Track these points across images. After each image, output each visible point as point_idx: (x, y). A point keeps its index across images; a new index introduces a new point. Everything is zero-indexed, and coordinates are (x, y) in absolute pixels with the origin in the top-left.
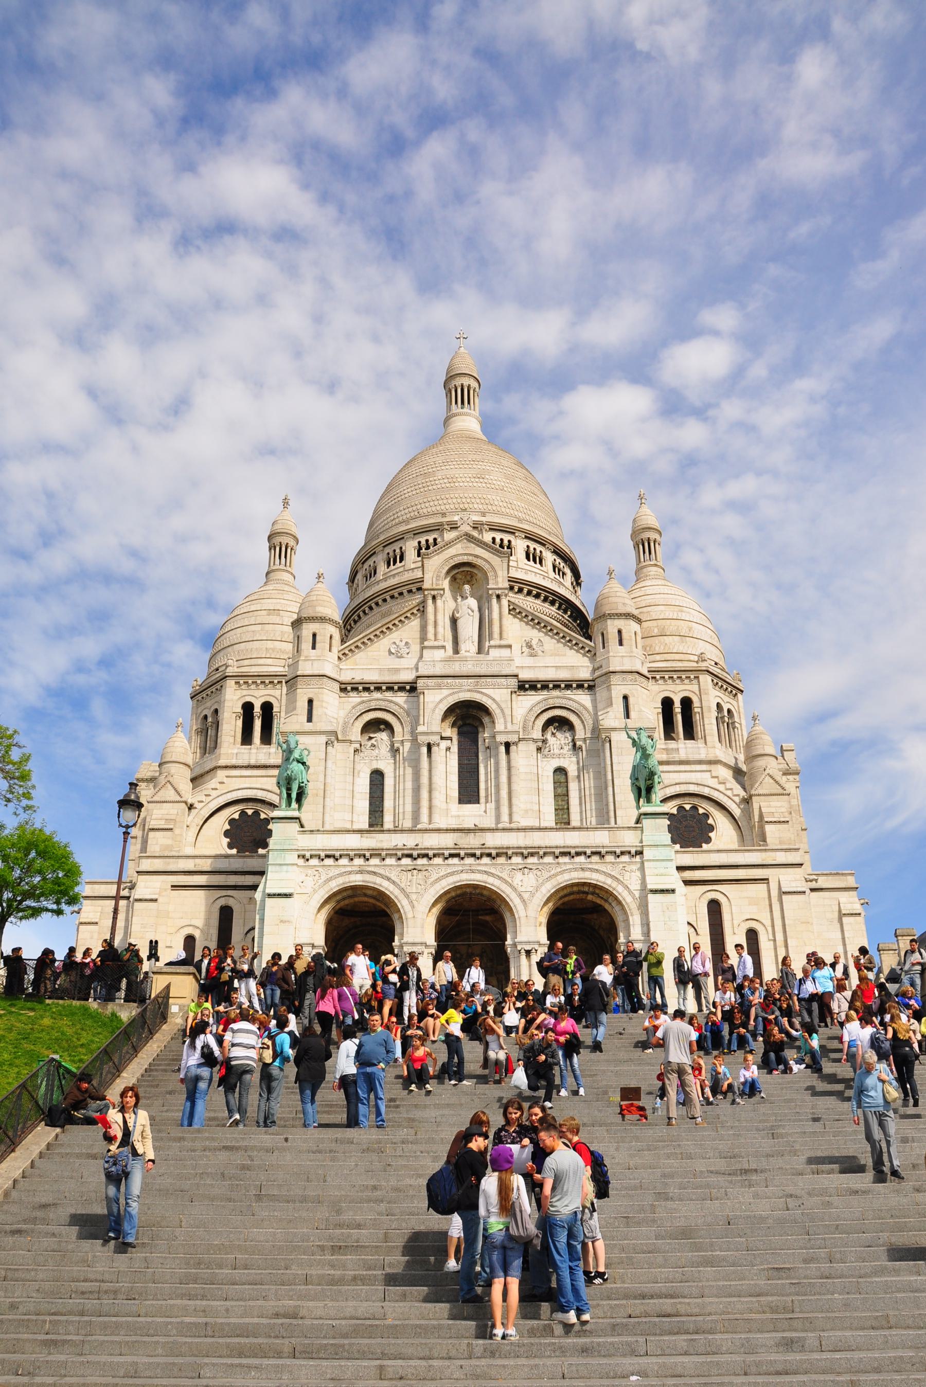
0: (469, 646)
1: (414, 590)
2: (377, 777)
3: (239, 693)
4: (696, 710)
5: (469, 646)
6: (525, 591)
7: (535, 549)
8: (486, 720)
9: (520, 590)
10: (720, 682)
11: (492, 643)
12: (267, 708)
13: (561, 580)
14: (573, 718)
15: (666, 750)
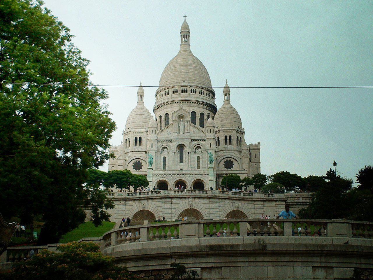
0: (182, 132)
1: (172, 103)
2: (165, 158)
3: (134, 135)
4: (232, 139)
5: (182, 132)
6: (199, 103)
7: (202, 91)
8: (185, 147)
9: (198, 103)
10: (238, 132)
11: (186, 132)
12: (140, 138)
13: (209, 97)
14: (201, 147)
15: (225, 148)
